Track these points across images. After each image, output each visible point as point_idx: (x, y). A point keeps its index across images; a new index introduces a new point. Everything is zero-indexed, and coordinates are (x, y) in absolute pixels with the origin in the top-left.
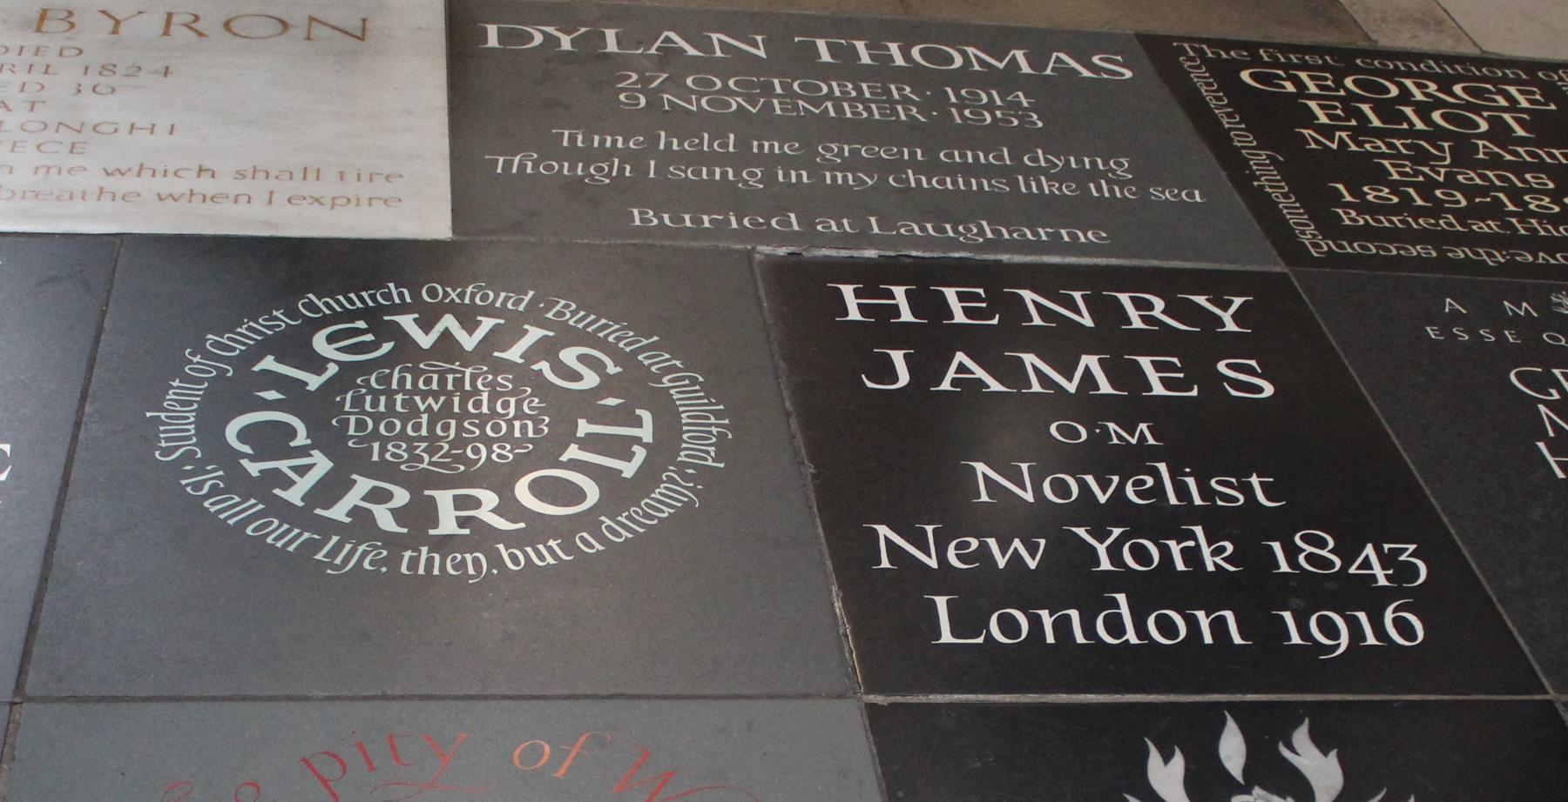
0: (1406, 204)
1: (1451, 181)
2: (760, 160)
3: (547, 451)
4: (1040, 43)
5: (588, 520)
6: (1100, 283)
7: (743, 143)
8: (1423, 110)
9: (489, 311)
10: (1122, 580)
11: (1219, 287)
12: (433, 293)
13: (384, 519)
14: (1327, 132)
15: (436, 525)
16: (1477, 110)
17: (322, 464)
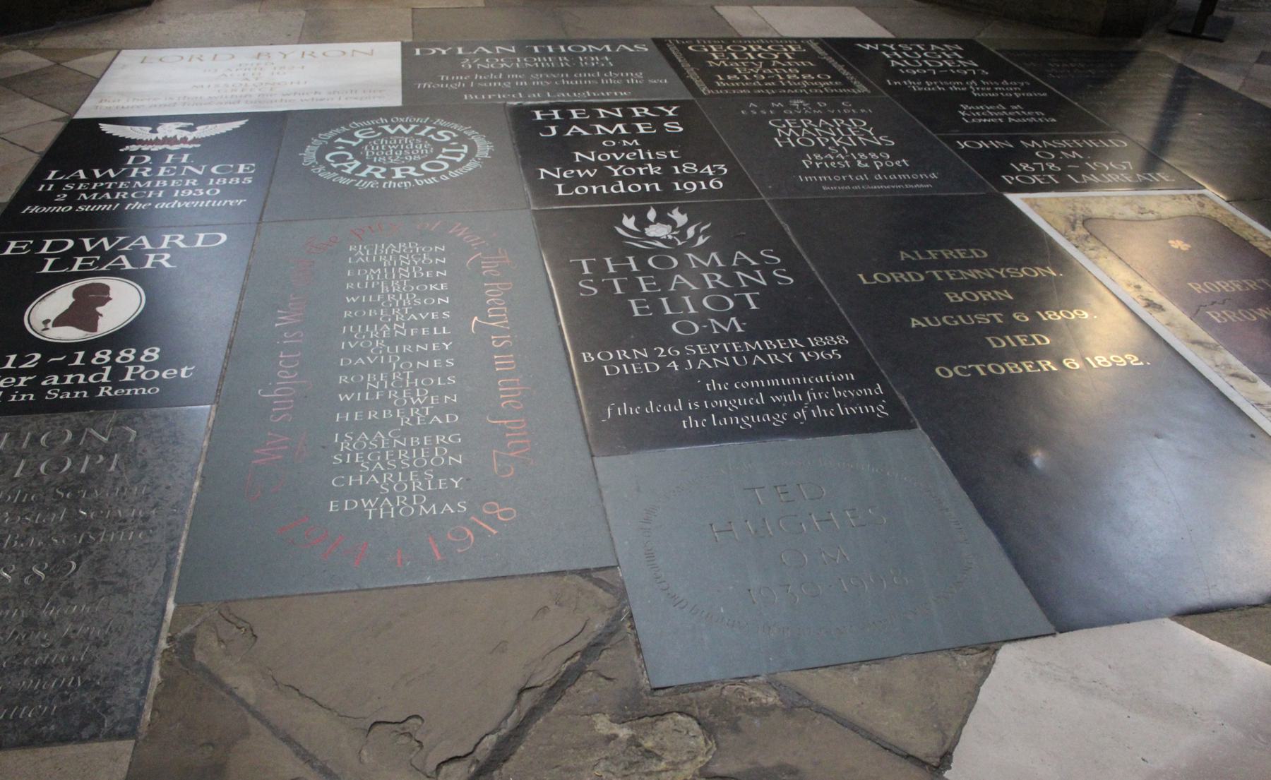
0: (742, 79)
1: (761, 72)
2: (511, 80)
3: (433, 156)
4: (614, 44)
5: (446, 172)
6: (626, 107)
7: (505, 76)
8: (755, 54)
9: (414, 123)
10: (622, 177)
11: (668, 104)
12: (395, 120)
13: (378, 175)
14: (718, 61)
15: (394, 175)
16: (776, 53)
17: (357, 163)
